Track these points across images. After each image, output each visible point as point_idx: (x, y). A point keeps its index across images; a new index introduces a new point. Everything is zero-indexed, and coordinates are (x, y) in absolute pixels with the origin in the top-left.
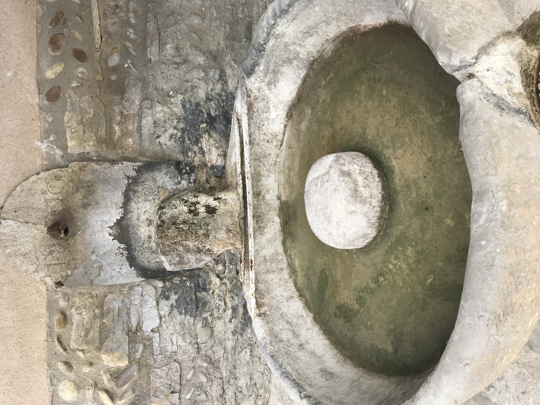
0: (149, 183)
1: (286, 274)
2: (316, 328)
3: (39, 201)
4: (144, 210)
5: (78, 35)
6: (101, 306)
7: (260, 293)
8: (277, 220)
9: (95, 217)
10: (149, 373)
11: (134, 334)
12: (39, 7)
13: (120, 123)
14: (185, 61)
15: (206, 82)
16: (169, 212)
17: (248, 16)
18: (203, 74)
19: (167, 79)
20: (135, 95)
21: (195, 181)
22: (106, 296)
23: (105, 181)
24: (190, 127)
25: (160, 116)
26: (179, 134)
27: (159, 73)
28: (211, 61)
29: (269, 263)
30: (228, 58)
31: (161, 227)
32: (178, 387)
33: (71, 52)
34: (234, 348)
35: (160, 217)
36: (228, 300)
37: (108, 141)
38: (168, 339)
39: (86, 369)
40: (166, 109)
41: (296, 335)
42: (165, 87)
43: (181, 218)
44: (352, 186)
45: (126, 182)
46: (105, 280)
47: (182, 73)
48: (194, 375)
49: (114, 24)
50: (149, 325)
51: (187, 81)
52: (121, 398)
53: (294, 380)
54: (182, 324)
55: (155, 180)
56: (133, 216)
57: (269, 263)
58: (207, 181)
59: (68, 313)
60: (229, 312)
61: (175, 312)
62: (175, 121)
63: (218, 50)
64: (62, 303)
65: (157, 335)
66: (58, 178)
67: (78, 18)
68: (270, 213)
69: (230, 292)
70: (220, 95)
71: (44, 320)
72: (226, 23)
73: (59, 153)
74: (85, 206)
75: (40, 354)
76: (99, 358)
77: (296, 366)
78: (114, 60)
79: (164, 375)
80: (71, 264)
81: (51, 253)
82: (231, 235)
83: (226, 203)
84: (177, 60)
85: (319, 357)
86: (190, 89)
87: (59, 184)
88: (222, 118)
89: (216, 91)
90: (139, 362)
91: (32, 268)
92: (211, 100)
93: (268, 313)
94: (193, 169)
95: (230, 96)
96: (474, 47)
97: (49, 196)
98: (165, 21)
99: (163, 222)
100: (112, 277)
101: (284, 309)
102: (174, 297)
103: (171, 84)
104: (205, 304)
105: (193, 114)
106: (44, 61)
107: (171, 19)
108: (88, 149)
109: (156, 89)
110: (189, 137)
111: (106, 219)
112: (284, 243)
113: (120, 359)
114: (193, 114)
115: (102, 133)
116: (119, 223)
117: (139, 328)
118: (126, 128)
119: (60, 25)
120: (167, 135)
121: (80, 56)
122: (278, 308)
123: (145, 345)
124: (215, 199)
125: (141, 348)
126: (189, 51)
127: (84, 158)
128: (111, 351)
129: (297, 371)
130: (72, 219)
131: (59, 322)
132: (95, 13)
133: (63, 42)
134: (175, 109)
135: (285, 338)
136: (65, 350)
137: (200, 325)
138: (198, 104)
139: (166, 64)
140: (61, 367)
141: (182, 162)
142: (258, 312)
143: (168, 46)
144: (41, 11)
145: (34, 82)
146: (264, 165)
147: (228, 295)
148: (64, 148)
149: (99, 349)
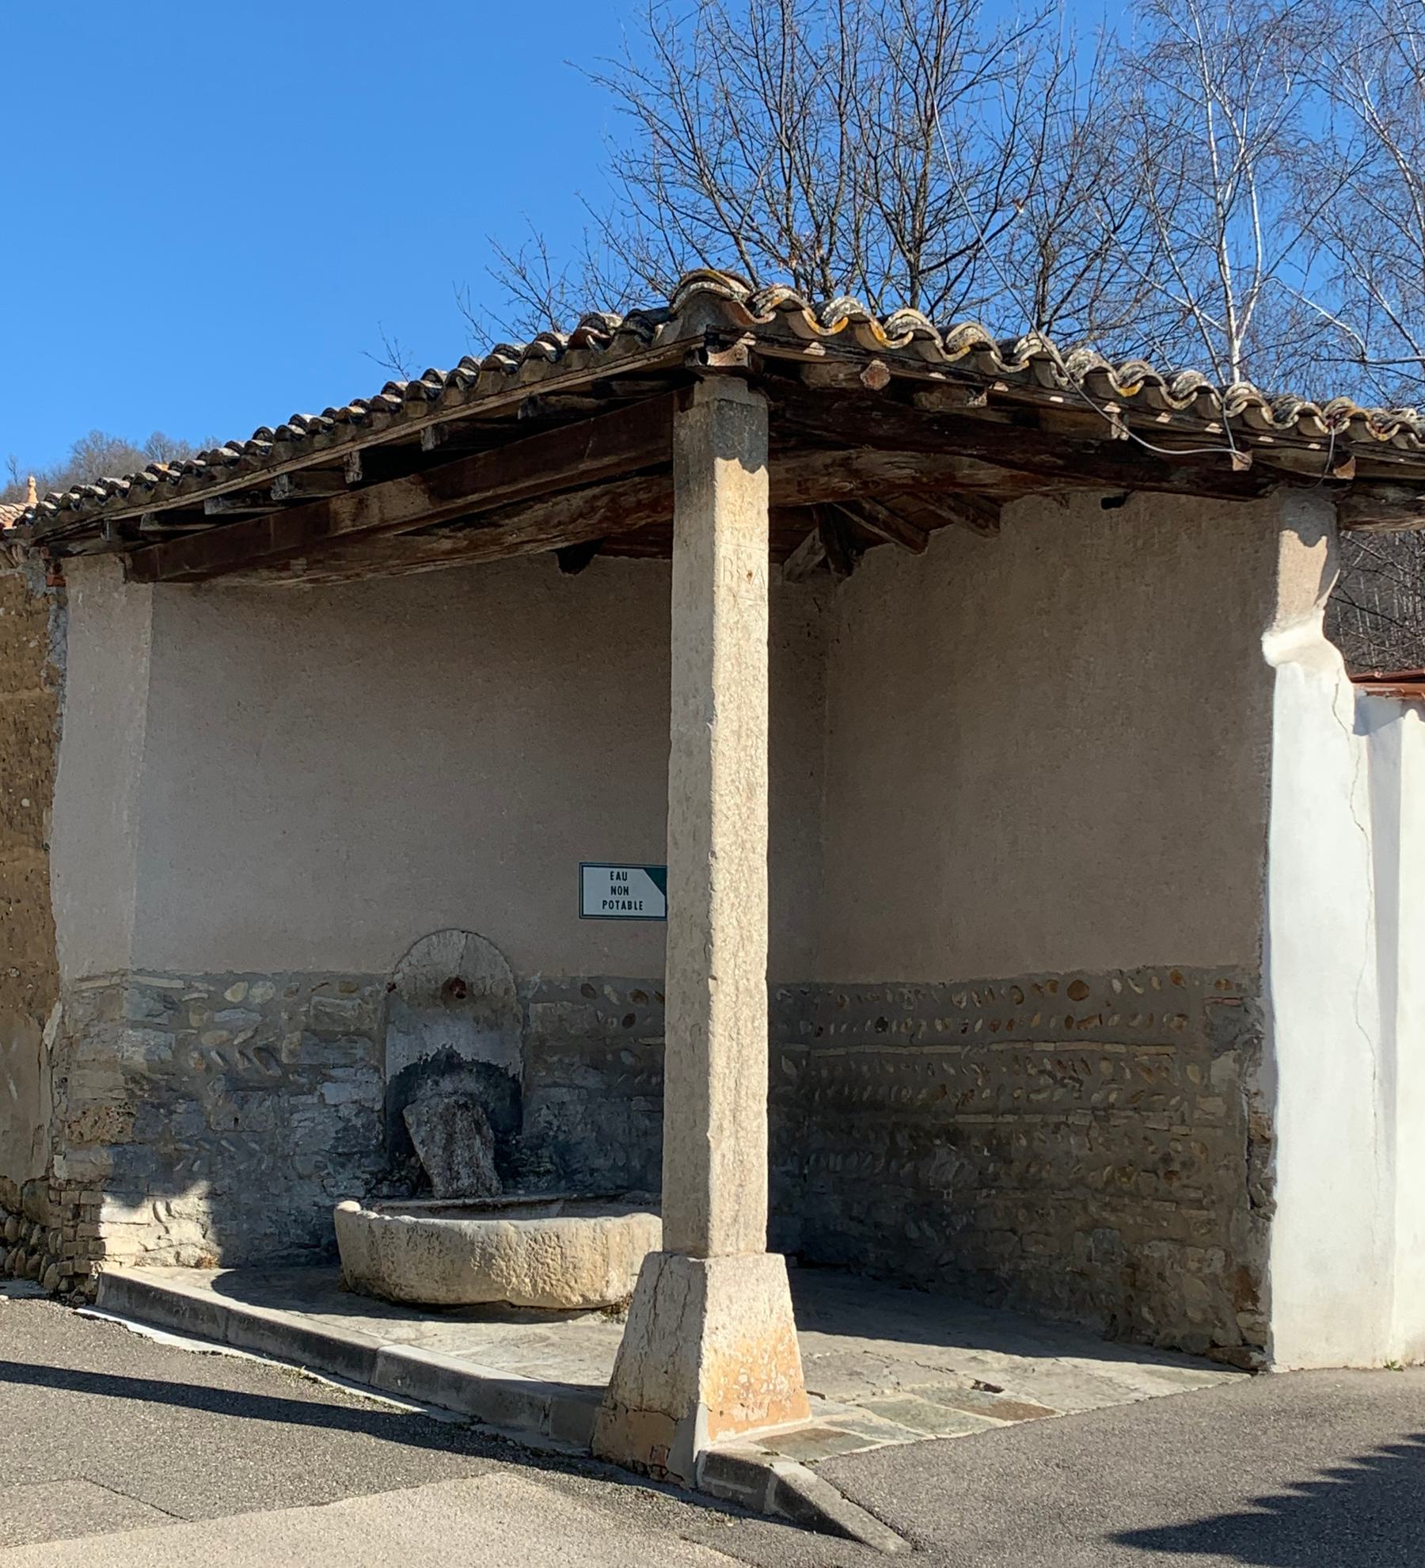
11: (321, 1073)
18: (620, 1164)
20: (593, 1081)
59: (354, 995)
61: (341, 1125)
65: (315, 1100)
71: (352, 970)
74: (476, 1020)
76: (297, 1029)
87: (501, 993)
97: (489, 981)
102: (358, 1122)
104: (343, 1166)
111: (462, 1041)
113: (292, 1053)
121: (629, 1020)
140: (294, 985)
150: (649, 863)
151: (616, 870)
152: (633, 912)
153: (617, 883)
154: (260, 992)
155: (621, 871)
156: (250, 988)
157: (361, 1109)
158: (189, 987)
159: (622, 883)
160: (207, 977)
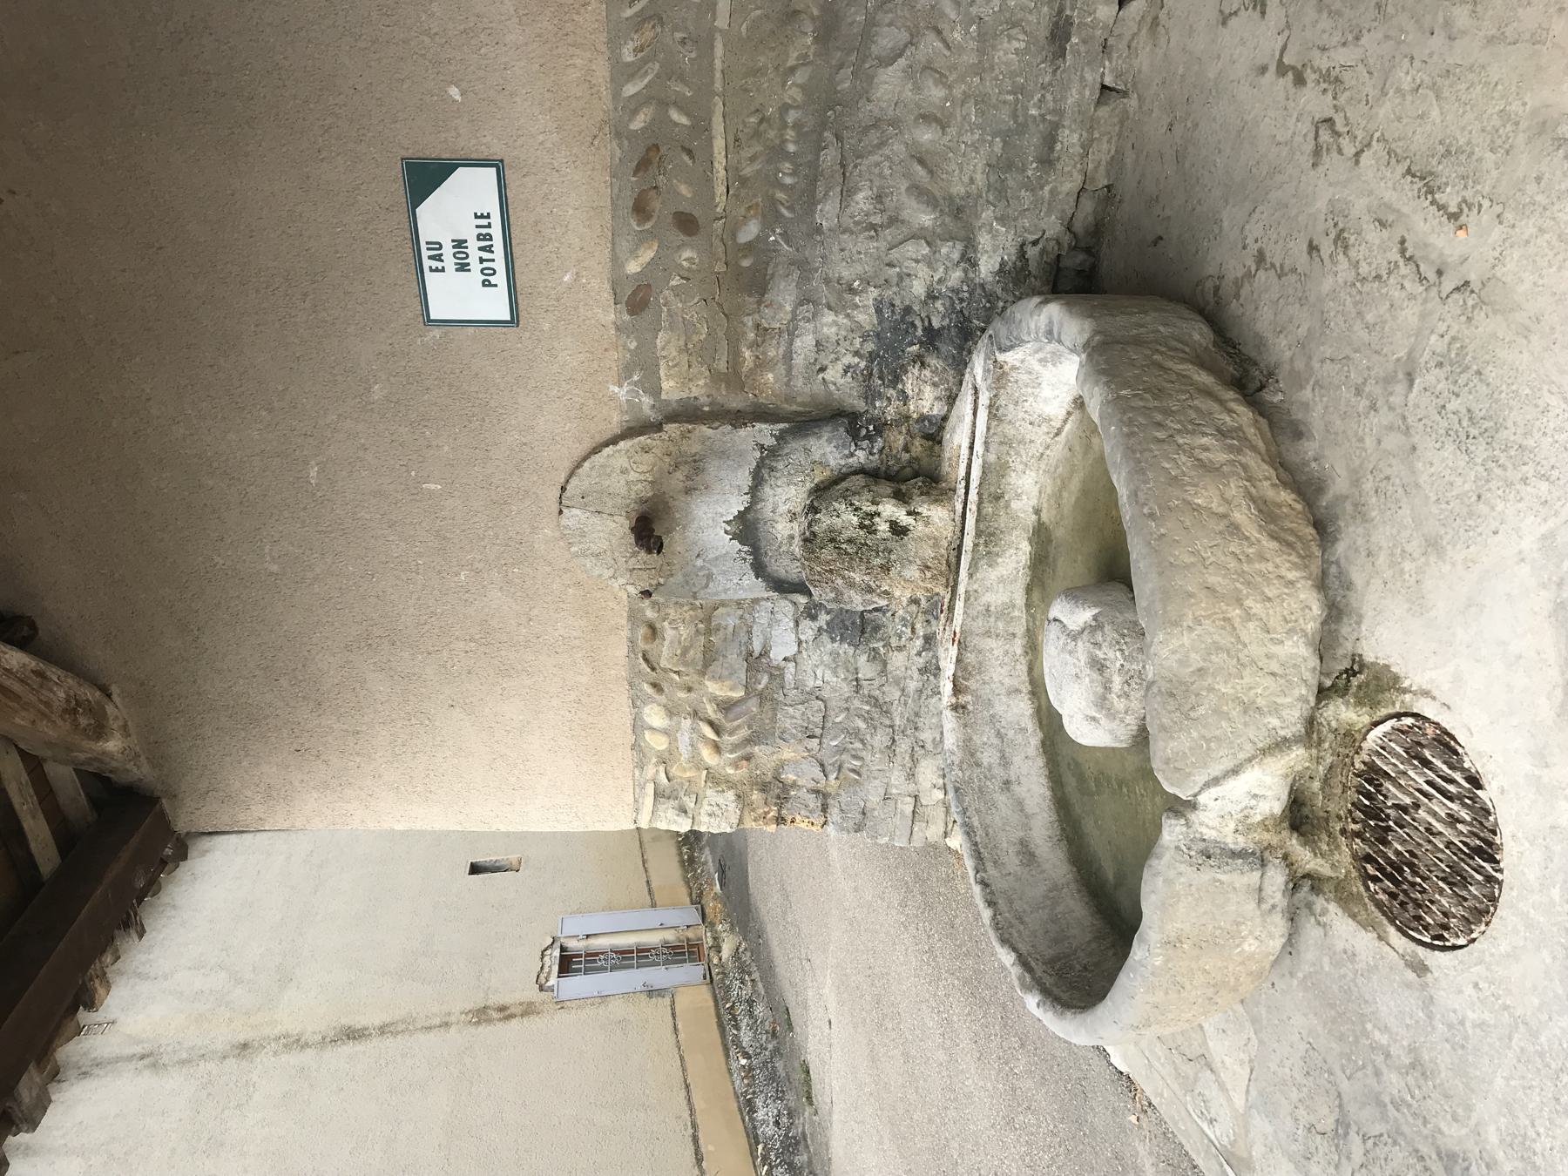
0: (798, 457)
1: (1018, 646)
2: (1041, 762)
3: (617, 484)
4: (786, 498)
5: (684, 190)
6: (708, 620)
7: (965, 669)
8: (1026, 547)
9: (705, 508)
10: (774, 709)
11: (756, 661)
12: (614, 144)
13: (754, 345)
14: (894, 221)
15: (930, 265)
16: (825, 521)
17: (1054, 112)
18: (926, 250)
19: (850, 259)
20: (784, 295)
21: (881, 451)
22: (716, 609)
23: (723, 454)
24: (886, 351)
25: (830, 331)
26: (863, 364)
27: (836, 248)
28: (948, 220)
29: (992, 619)
30: (987, 214)
31: (809, 540)
32: (818, 732)
33: (670, 219)
35: (810, 525)
36: (918, 626)
37: (733, 378)
38: (810, 671)
39: (682, 695)
40: (841, 319)
41: (1005, 762)
42: (845, 274)
43: (846, 535)
44: (1100, 690)
45: (758, 454)
46: (716, 594)
47: (883, 245)
48: (847, 718)
49: (753, 159)
50: (777, 654)
51: (890, 265)
52: (731, 734)
53: (976, 844)
54: (835, 655)
55: (807, 451)
56: (766, 509)
57: (992, 619)
58: (906, 449)
59: (658, 626)
60: (919, 643)
61: (825, 637)
62: (859, 340)
63: (968, 195)
66: (646, 450)
67: (686, 158)
68: (1015, 533)
69: (925, 613)
70: (957, 291)
71: (625, 633)
72: (994, 135)
73: (647, 401)
74: (688, 491)
75: (617, 650)
77: (989, 819)
78: (750, 231)
79: (798, 714)
81: (634, 554)
82: (929, 575)
83: (927, 524)
84: (877, 219)
85: (1027, 817)
86: (895, 280)
87: (649, 458)
88: (953, 332)
89: (950, 284)
90: (760, 695)
91: (608, 573)
92: (935, 298)
93: (970, 708)
94: (881, 427)
95: (979, 291)
96: (1201, 779)
97: (633, 476)
98: (860, 141)
99: (814, 534)
100: (726, 590)
101: (999, 708)
103: (859, 269)
105: (895, 330)
106: (624, 243)
107: (874, 137)
108: (695, 392)
109: (827, 281)
110: (881, 371)
112: (1029, 590)
114: (895, 330)
115: (722, 366)
116: (741, 516)
117: (765, 653)
118: (764, 353)
119: (653, 169)
120: (840, 367)
121: (687, 224)
122: (990, 703)
123: (771, 675)
124: (909, 513)
125: (765, 679)
126: (904, 198)
127: (688, 414)
129: (986, 828)
130: (667, 509)
131: (645, 638)
132: (719, 144)
133: (656, 205)
134: (861, 317)
135: (985, 762)
136: (653, 669)
137: (864, 658)
138: (908, 310)
139: (852, 233)
141: (861, 415)
142: (954, 700)
143: (860, 196)
144: (618, 152)
145: (607, 286)
146: (1018, 453)
147: (921, 617)
148: (655, 391)
149: (703, 673)
150: (397, 189)
151: (427, 263)
152: (496, 220)
153: (449, 261)
154: (655, 716)
155: (425, 254)
156: (652, 729)
159: (448, 251)
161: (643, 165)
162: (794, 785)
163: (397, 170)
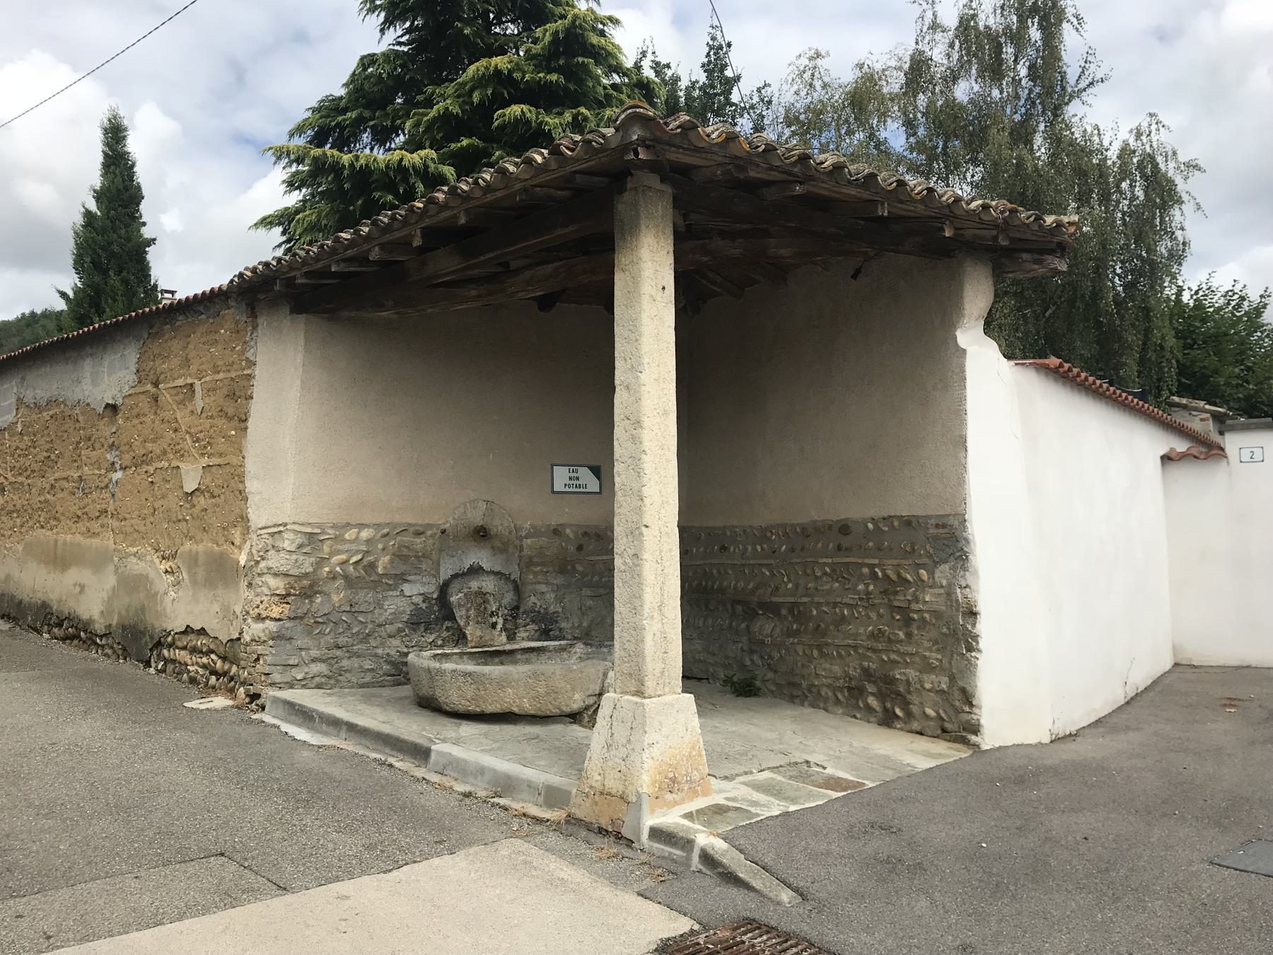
3: (497, 522)
4: (488, 584)
11: (402, 578)
14: (583, 614)
20: (559, 580)
34: (376, 655)
39: (380, 546)
64: (429, 533)
66: (510, 533)
71: (420, 522)
74: (493, 548)
78: (580, 568)
80: (456, 538)
102: (424, 606)
104: (415, 630)
115: (535, 560)
121: (580, 548)
128: (391, 562)
140: (386, 531)
149: (394, 554)
150: (593, 463)
153: (572, 475)
154: (365, 534)
157: (426, 598)
158: (323, 532)
160: (334, 527)
161: (598, 536)
162: (311, 602)
163: (598, 464)
